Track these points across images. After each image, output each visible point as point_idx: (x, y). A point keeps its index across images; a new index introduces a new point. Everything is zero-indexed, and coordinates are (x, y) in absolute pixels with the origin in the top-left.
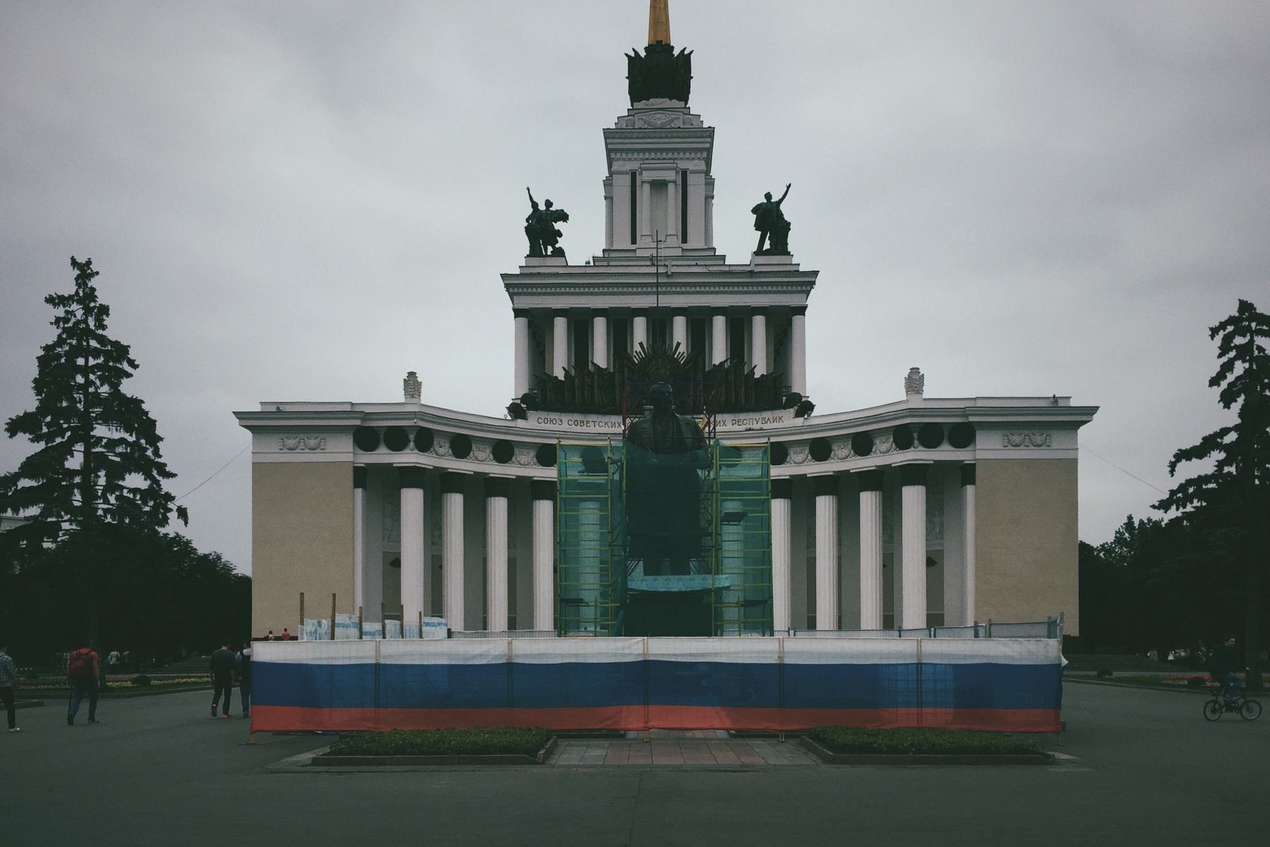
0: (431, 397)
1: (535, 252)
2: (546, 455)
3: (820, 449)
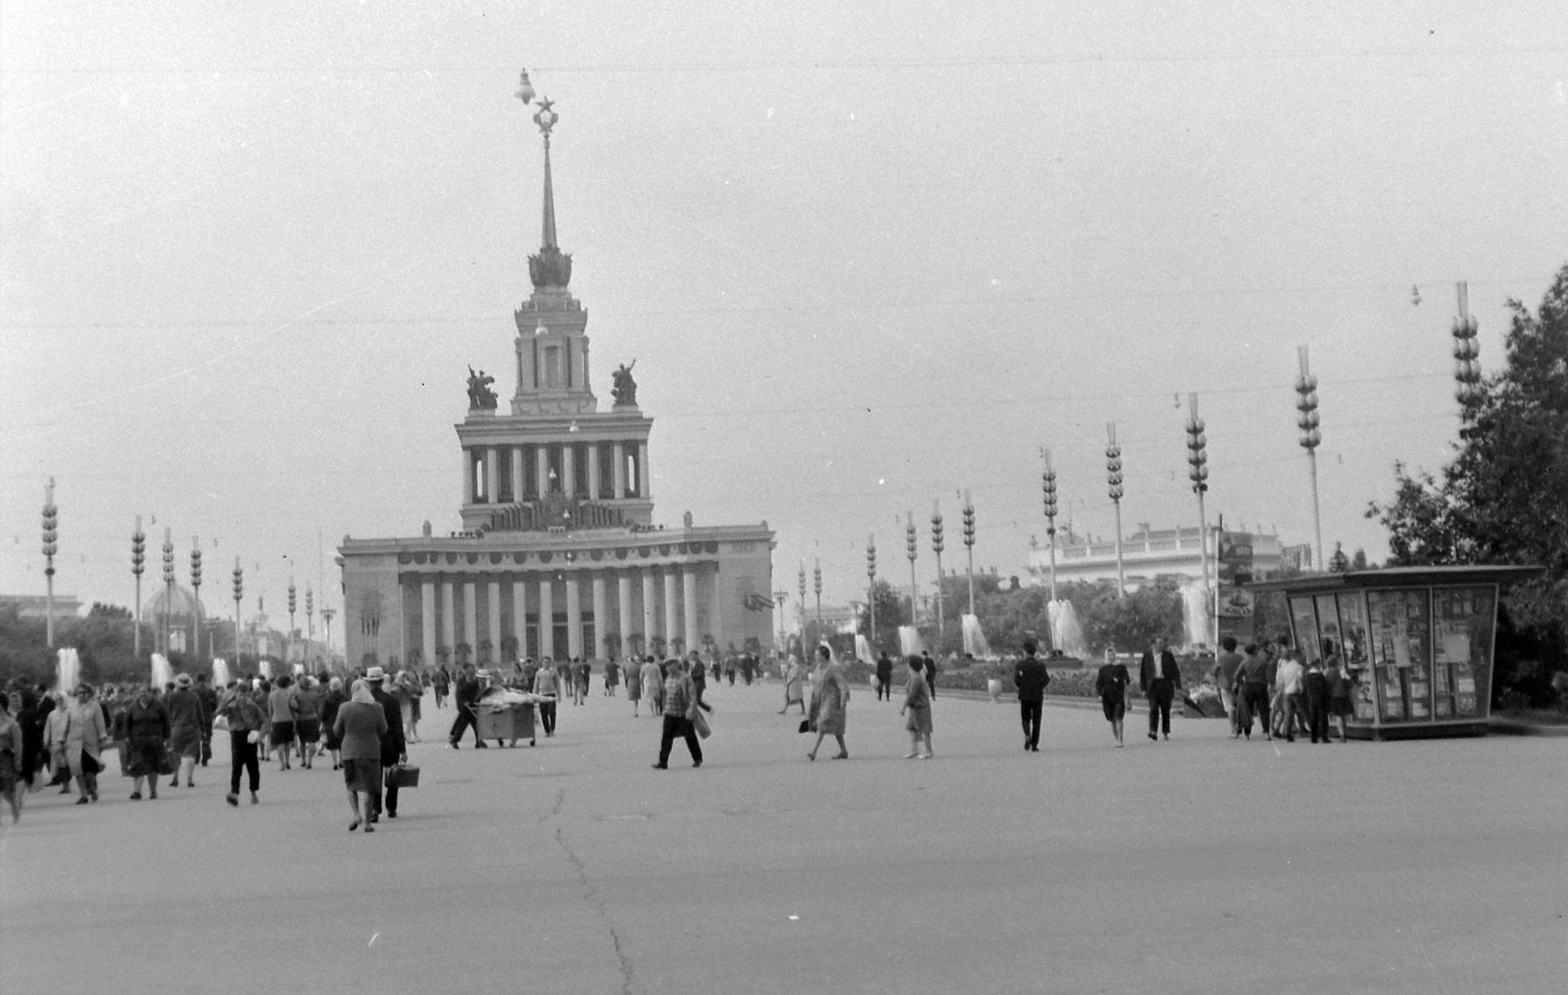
0: (434, 534)
1: (474, 406)
2: (496, 558)
3: (644, 552)
